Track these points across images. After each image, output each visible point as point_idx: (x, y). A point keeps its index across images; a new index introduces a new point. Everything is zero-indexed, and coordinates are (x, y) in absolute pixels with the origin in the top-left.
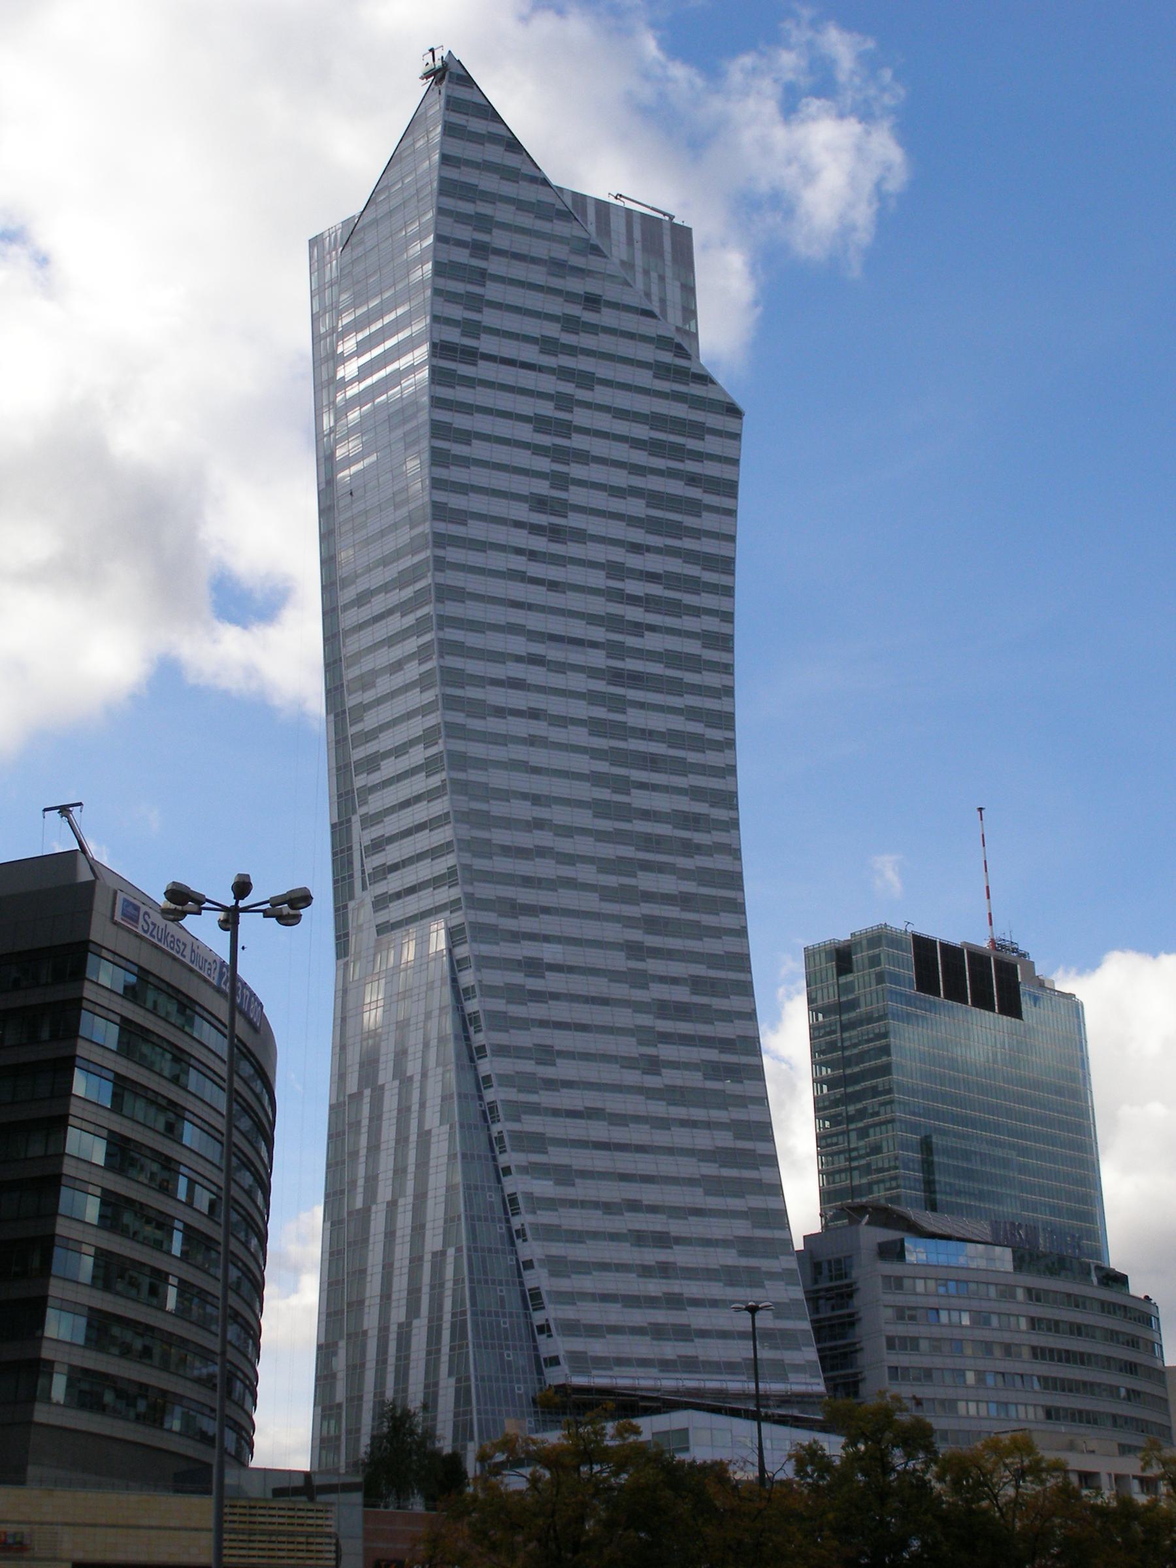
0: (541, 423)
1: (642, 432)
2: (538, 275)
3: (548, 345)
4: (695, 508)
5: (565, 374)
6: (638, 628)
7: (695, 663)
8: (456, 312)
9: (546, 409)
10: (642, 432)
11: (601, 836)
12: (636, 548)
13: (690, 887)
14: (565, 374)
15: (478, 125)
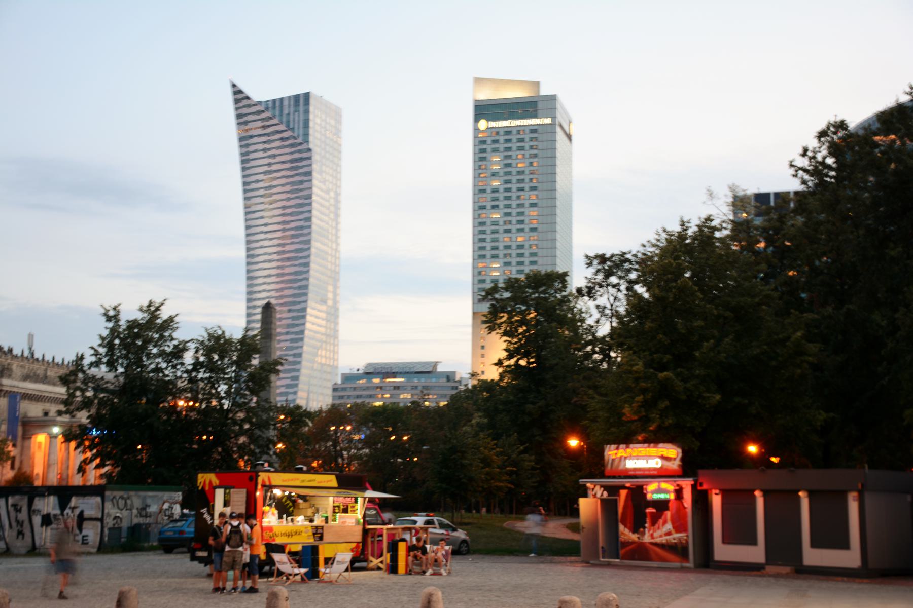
0: (266, 173)
1: (288, 165)
2: (260, 132)
3: (265, 150)
4: (302, 182)
5: (269, 157)
6: (288, 222)
7: (301, 228)
8: (245, 150)
9: (266, 168)
10: (288, 165)
11: (277, 283)
12: (288, 199)
13: (296, 292)
14: (269, 157)
15: (240, 96)
